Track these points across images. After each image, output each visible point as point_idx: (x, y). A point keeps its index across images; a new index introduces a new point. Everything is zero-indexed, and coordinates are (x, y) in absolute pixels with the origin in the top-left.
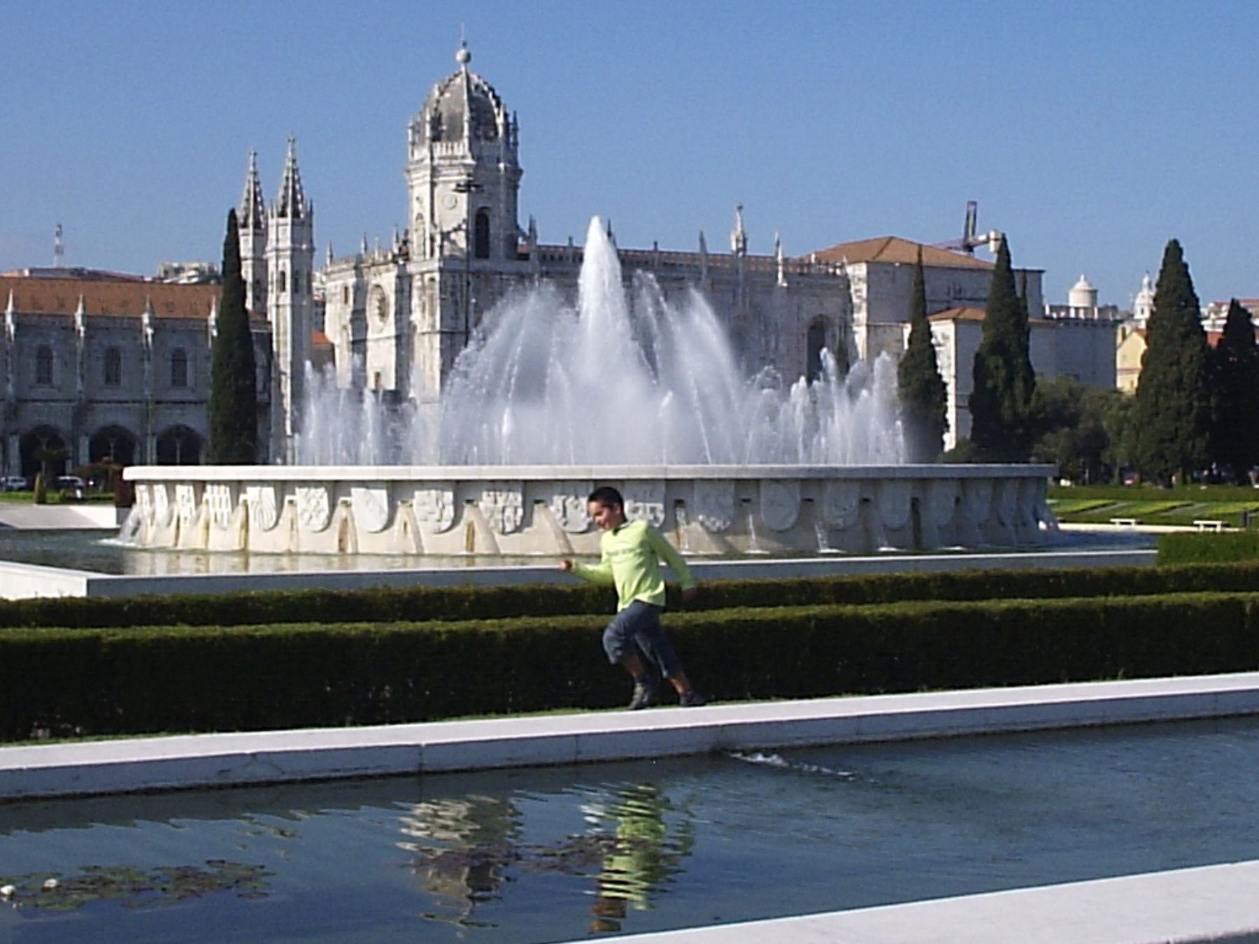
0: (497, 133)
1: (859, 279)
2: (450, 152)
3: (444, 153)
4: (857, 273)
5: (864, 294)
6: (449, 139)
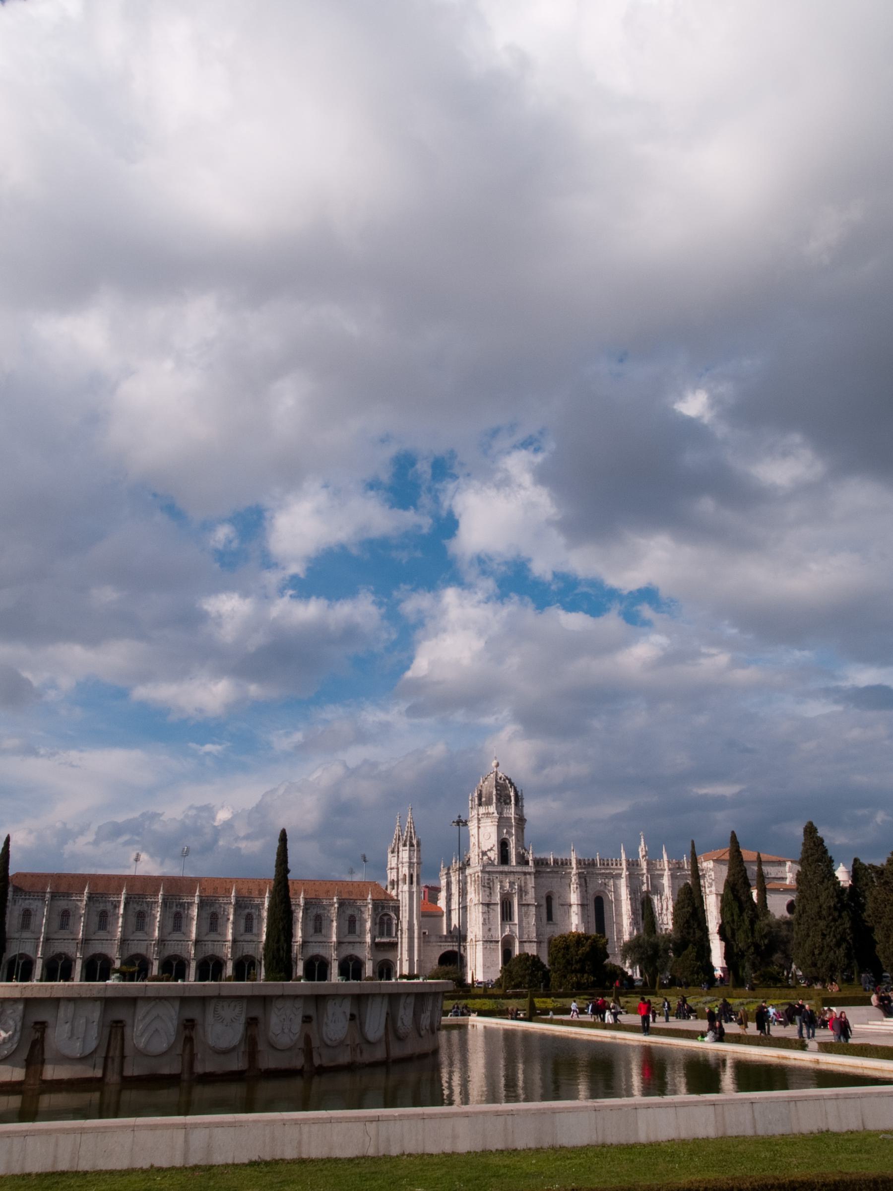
0: (511, 801)
1: (710, 869)
2: (487, 811)
3: (484, 812)
4: (709, 866)
5: (713, 877)
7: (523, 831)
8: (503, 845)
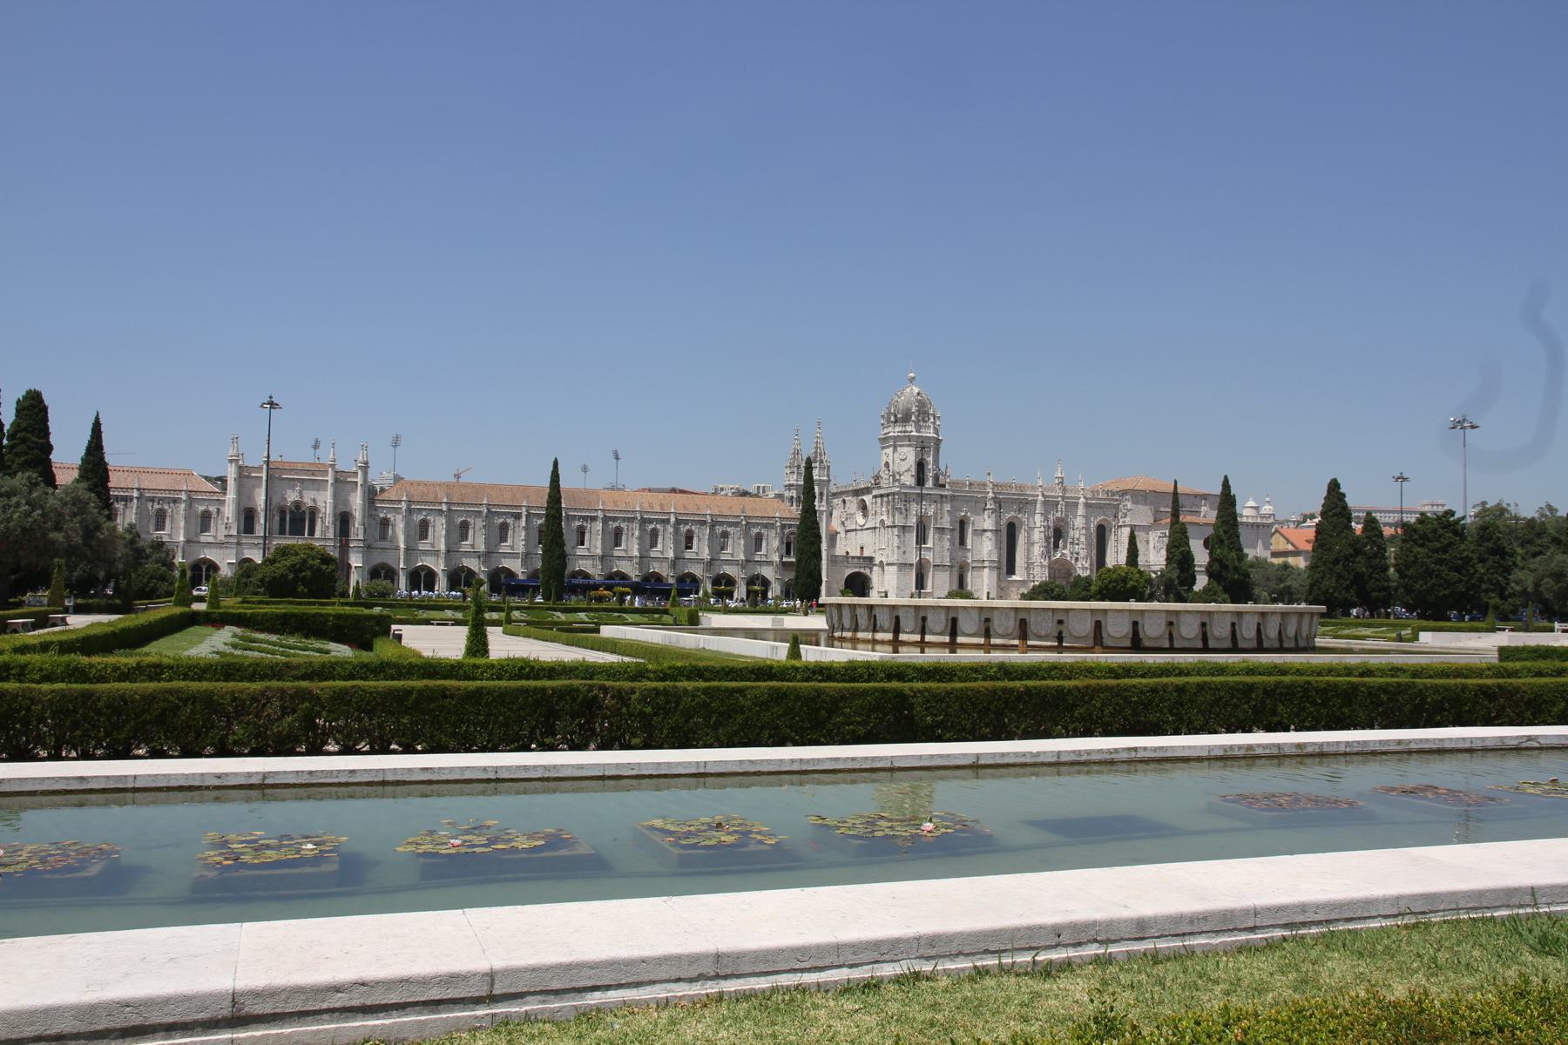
0: (929, 419)
6: (903, 422)
7: (938, 451)
8: (921, 466)
